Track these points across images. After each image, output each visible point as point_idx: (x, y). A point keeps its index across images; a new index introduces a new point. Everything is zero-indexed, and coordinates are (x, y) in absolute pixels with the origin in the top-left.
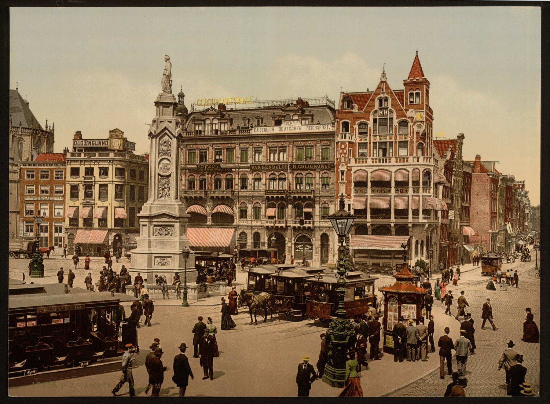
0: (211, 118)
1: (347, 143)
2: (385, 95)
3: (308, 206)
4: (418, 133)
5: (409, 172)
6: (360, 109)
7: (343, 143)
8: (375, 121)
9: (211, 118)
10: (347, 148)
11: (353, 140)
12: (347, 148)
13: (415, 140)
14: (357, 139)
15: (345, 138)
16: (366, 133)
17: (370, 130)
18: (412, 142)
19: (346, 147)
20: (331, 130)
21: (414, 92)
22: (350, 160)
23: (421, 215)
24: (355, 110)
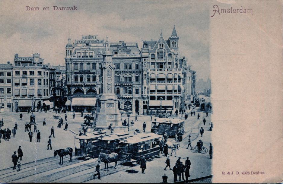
0: (85, 50)
1: (147, 62)
2: (162, 43)
3: (130, 88)
5: (172, 74)
6: (152, 48)
7: (146, 62)
8: (158, 53)
9: (85, 50)
11: (149, 61)
12: (147, 64)
13: (174, 62)
15: (146, 60)
16: (154, 58)
17: (156, 57)
18: (173, 62)
21: (174, 42)
22: (148, 69)
23: (178, 92)
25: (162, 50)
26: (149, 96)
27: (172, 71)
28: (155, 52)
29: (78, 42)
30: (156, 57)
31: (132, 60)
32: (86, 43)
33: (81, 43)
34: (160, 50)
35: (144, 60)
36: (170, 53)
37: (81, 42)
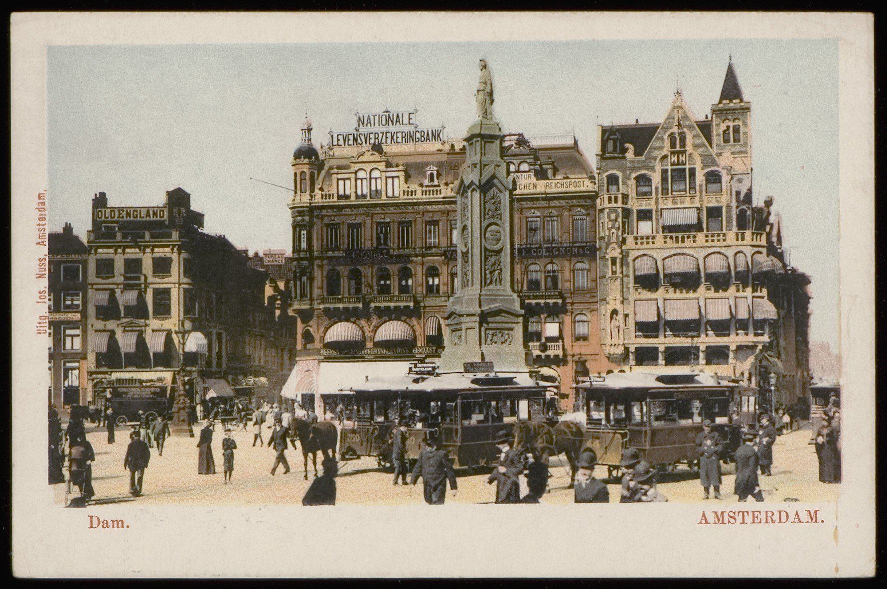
1: (620, 210)
4: (738, 193)
7: (614, 210)
10: (620, 220)
13: (734, 204)
14: (635, 205)
19: (617, 216)
20: (591, 189)
24: (630, 155)
25: (682, 158)
26: (632, 349)
27: (725, 244)
28: (653, 169)
29: (341, 137)
30: (657, 188)
31: (563, 202)
32: (372, 141)
33: (351, 142)
34: (675, 159)
35: (610, 202)
36: (713, 168)
37: (351, 137)
